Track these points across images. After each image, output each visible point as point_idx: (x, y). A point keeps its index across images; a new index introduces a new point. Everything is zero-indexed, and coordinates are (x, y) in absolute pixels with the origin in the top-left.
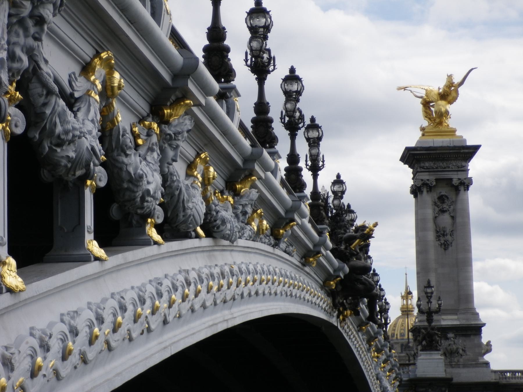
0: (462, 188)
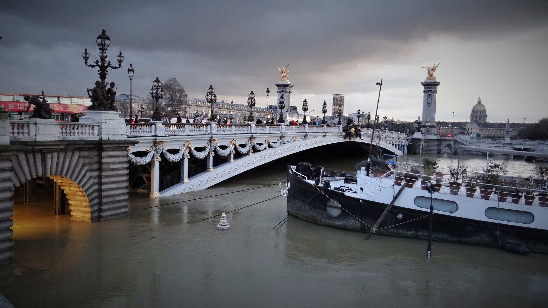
0: (435, 92)
